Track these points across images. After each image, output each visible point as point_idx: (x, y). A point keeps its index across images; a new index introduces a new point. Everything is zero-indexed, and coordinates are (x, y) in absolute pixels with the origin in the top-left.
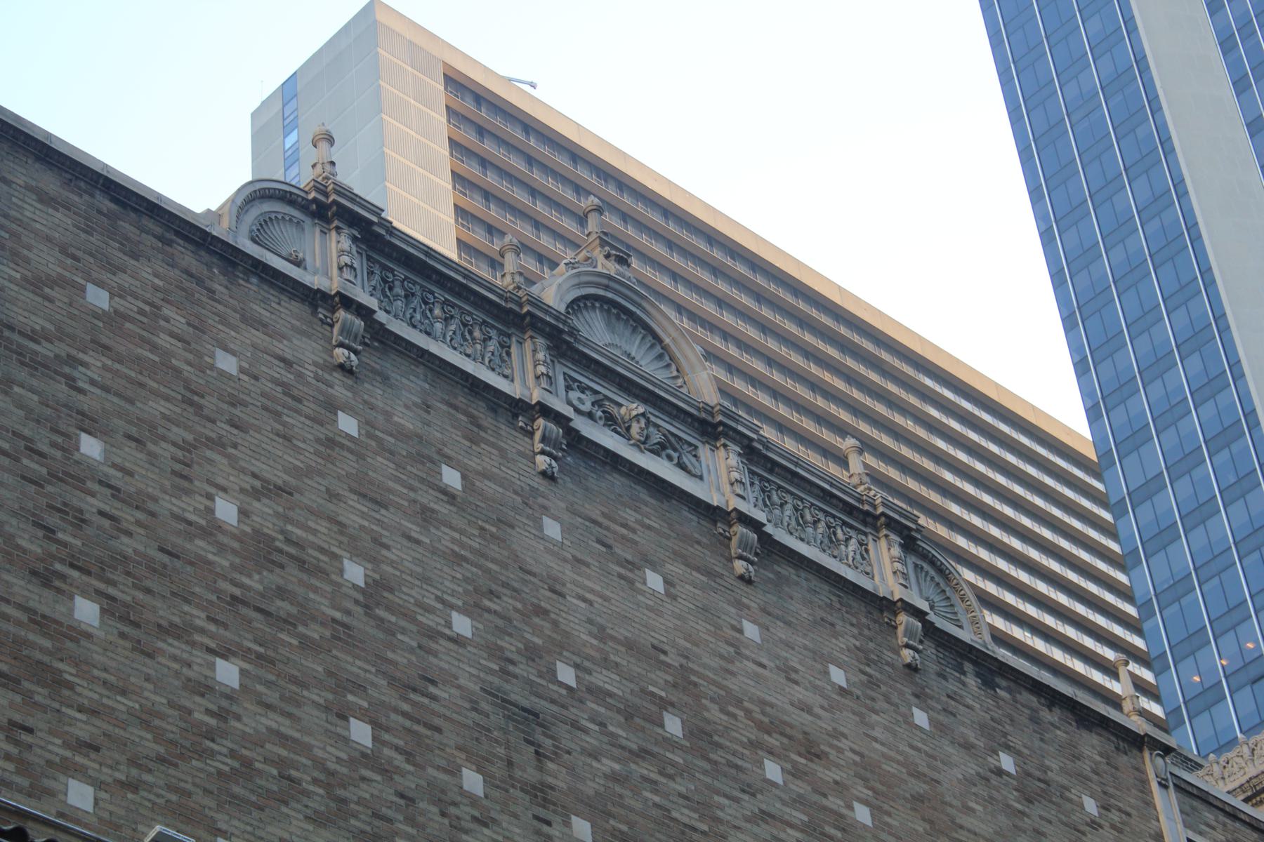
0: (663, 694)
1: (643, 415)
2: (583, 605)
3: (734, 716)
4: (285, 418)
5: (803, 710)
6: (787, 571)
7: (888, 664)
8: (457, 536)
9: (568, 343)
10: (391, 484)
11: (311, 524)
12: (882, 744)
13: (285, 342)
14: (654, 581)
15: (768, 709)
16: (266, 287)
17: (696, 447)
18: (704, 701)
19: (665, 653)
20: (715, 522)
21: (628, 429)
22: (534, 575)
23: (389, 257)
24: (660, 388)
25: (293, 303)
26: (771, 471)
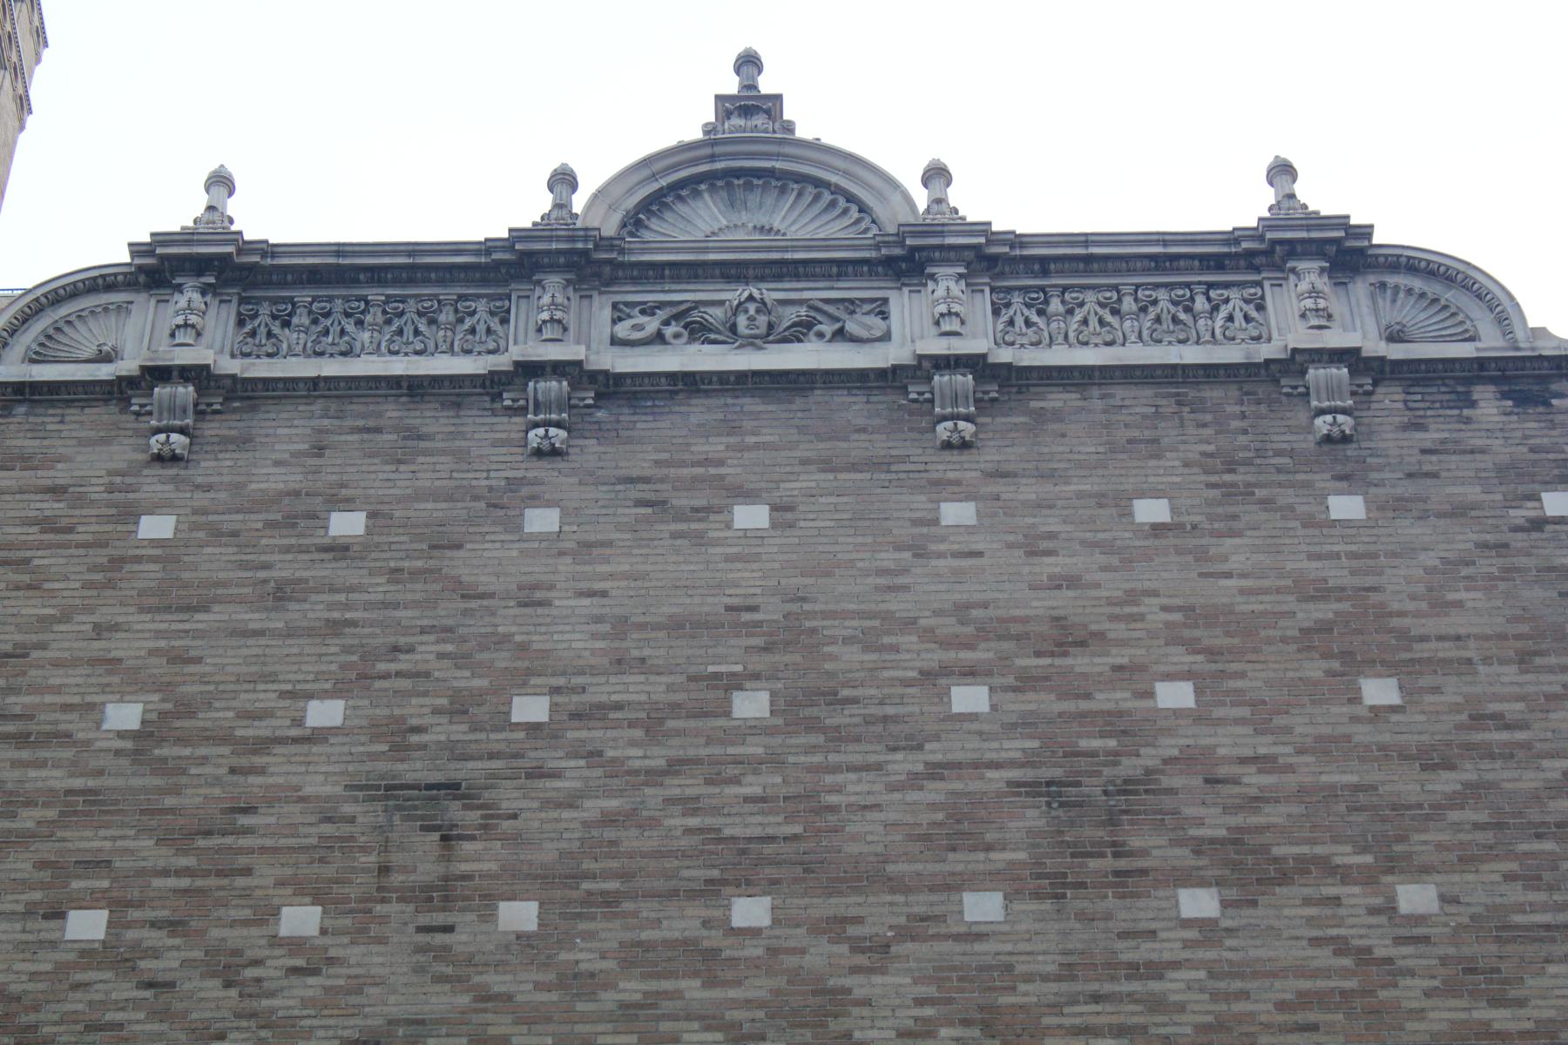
0: (739, 668)
1: (751, 298)
2: (586, 602)
3: (895, 649)
4: (36, 562)
5: (1059, 587)
6: (1056, 400)
7: (1279, 453)
8: (342, 597)
9: (610, 262)
10: (222, 575)
11: (52, 681)
12: (1243, 576)
13: (59, 466)
14: (751, 517)
15: (976, 613)
16: (40, 411)
17: (885, 301)
18: (827, 649)
19: (753, 609)
20: (904, 390)
21: (733, 328)
22: (492, 595)
23: (283, 284)
24: (795, 249)
25: (87, 411)
26: (1045, 273)
